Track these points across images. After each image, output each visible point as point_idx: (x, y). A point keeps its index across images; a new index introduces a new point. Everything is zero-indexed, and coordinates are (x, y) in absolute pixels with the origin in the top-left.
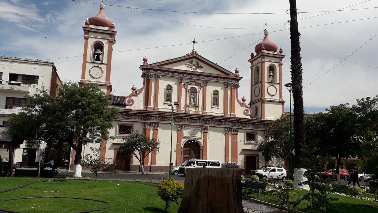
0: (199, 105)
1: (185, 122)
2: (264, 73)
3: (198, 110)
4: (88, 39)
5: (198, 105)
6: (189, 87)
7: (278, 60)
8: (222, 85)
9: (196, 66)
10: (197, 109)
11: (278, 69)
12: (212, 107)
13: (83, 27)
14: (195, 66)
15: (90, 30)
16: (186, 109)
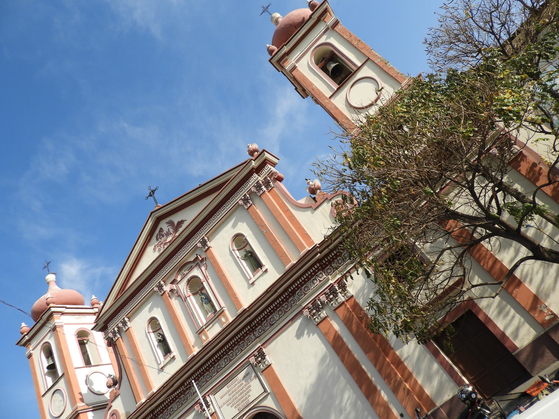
0: (222, 306)
1: (207, 381)
2: (311, 84)
3: (227, 319)
4: (31, 355)
5: (221, 307)
6: (183, 287)
7: (321, 28)
8: (239, 213)
9: (171, 230)
10: (223, 320)
11: (333, 41)
12: (251, 282)
13: (17, 344)
14: (171, 234)
15: (27, 338)
16: (202, 341)
